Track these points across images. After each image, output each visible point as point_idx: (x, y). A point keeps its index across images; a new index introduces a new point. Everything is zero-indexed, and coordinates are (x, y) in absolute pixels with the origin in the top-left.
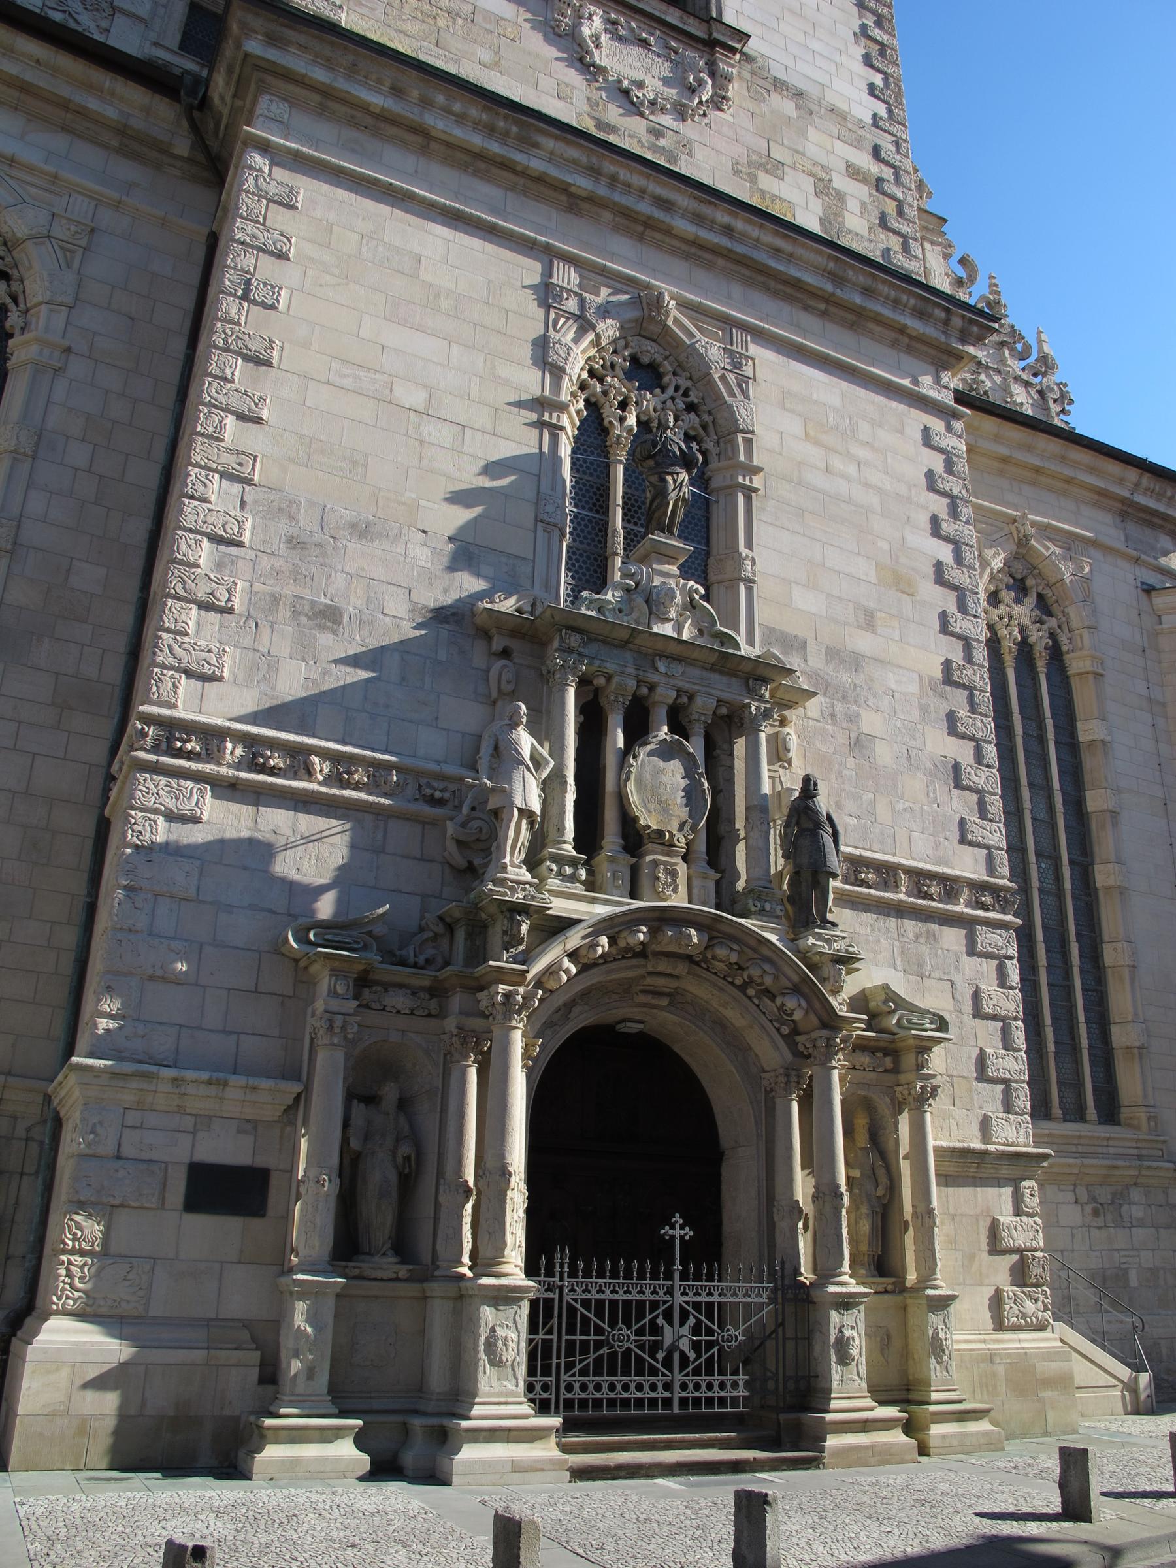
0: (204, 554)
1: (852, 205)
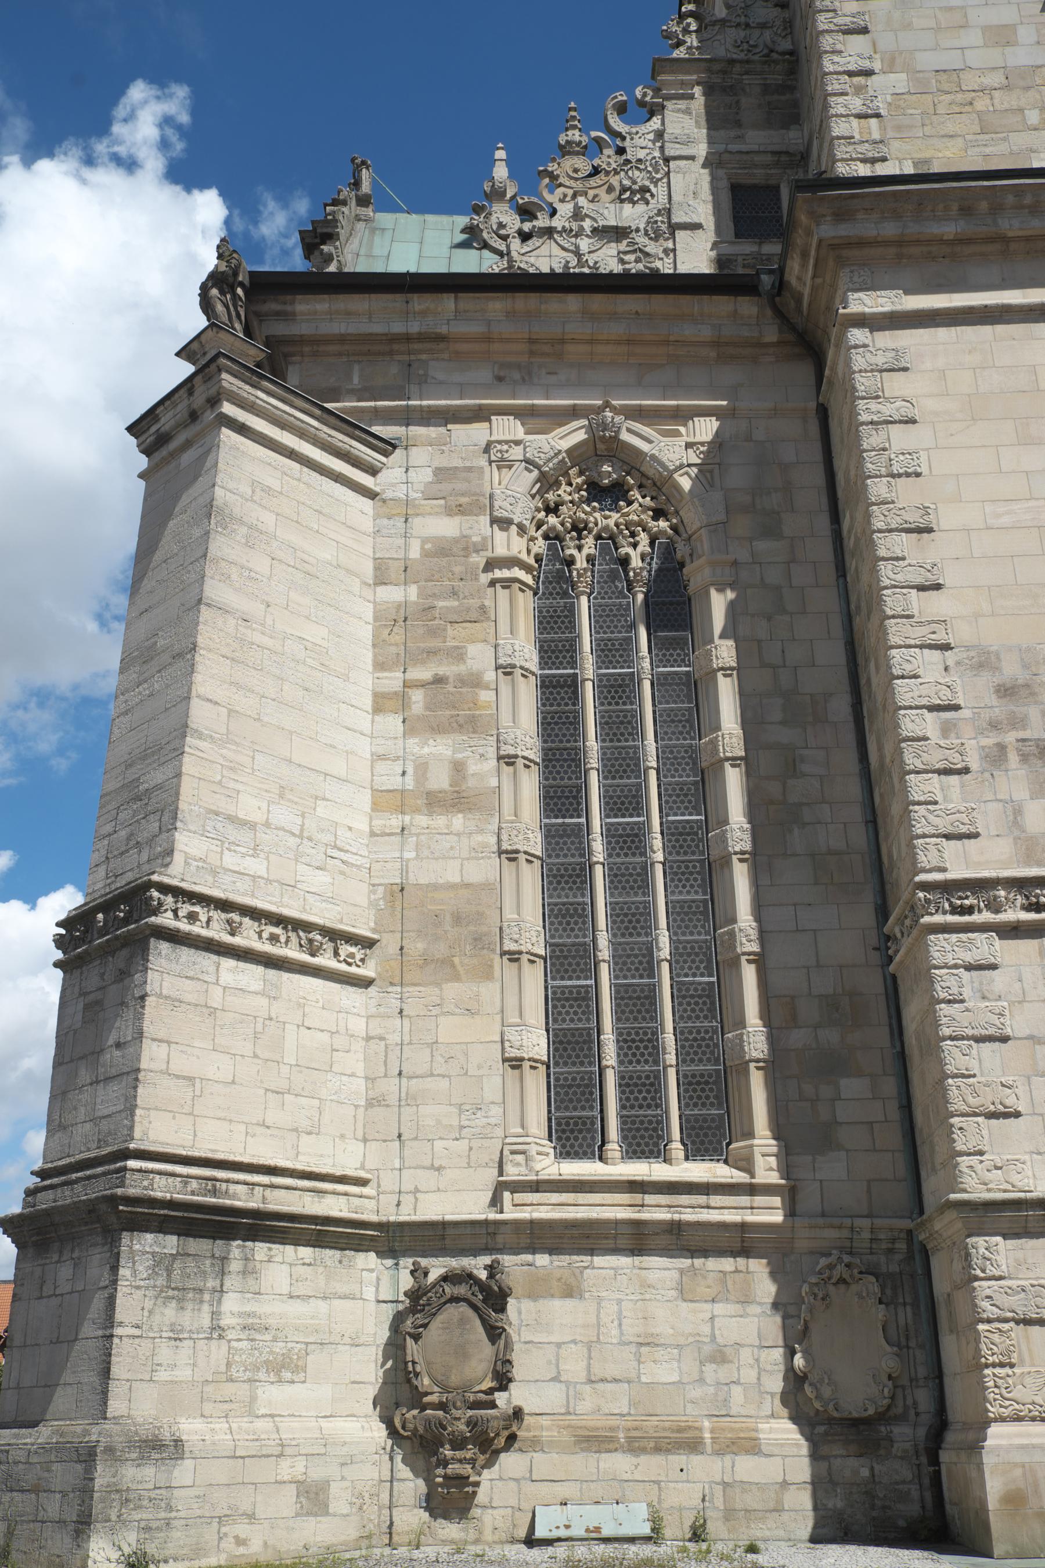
0: (929, 724)
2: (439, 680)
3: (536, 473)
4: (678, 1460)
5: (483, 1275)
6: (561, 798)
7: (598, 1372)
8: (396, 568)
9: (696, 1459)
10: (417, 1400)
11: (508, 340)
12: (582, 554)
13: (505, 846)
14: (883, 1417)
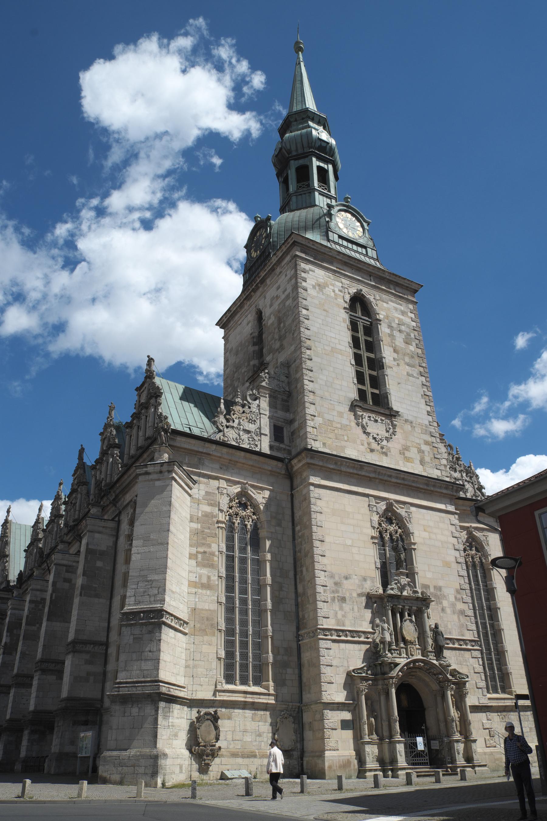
1: (426, 453)
2: (205, 552)
3: (229, 498)
4: (252, 759)
5: (213, 713)
6: (230, 588)
7: (235, 738)
8: (195, 518)
9: (256, 759)
10: (198, 744)
11: (225, 459)
12: (237, 521)
13: (219, 601)
14: (291, 750)
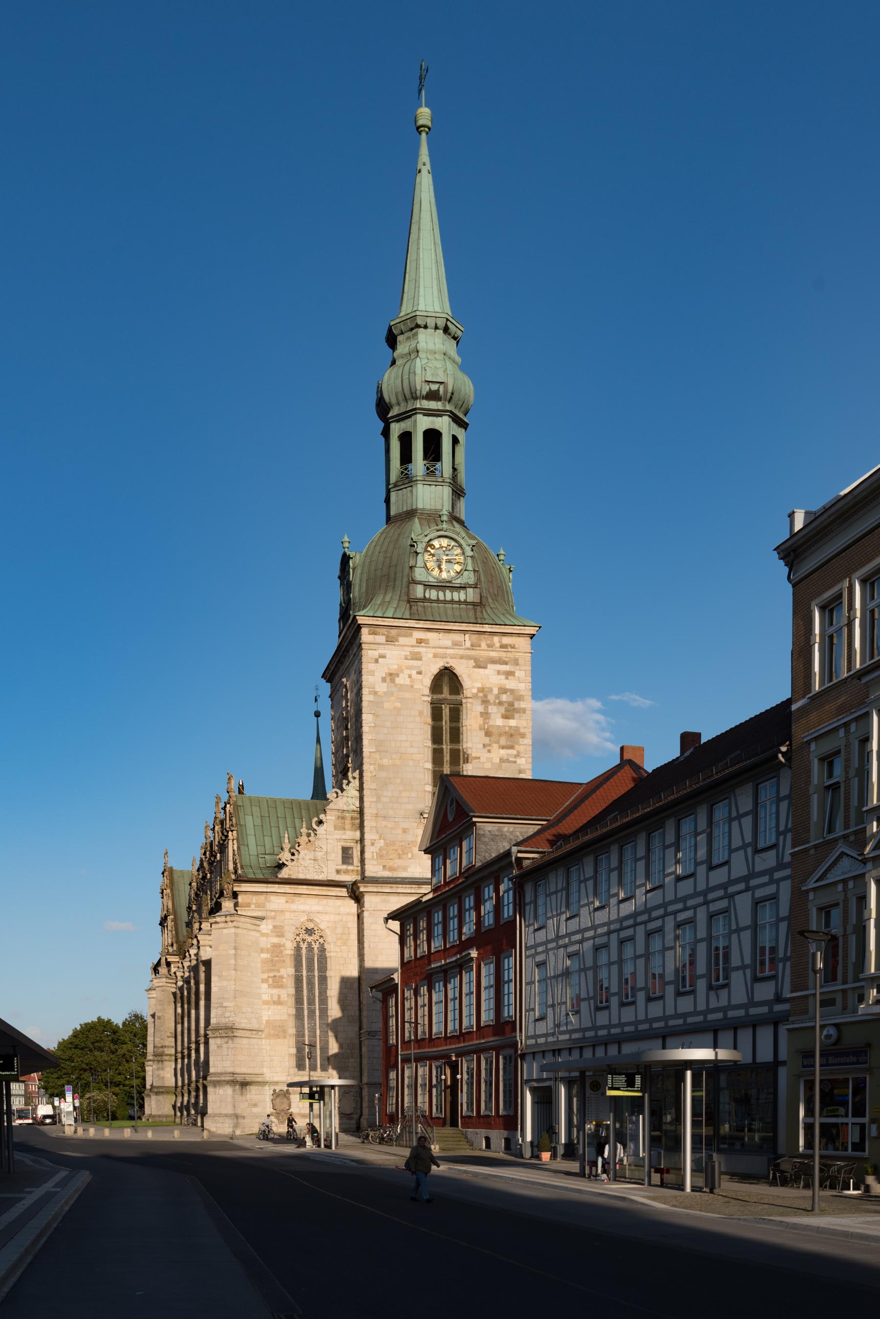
2: (275, 976)
12: (304, 946)
